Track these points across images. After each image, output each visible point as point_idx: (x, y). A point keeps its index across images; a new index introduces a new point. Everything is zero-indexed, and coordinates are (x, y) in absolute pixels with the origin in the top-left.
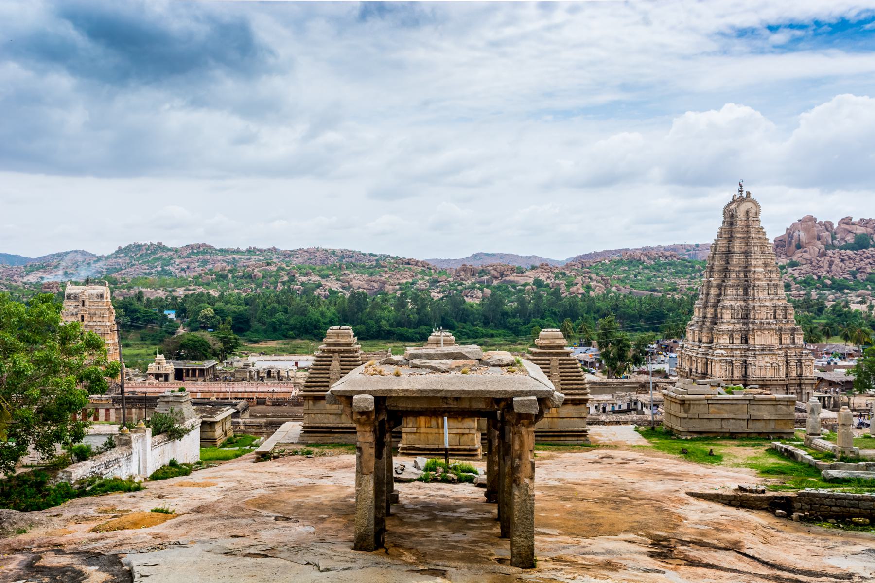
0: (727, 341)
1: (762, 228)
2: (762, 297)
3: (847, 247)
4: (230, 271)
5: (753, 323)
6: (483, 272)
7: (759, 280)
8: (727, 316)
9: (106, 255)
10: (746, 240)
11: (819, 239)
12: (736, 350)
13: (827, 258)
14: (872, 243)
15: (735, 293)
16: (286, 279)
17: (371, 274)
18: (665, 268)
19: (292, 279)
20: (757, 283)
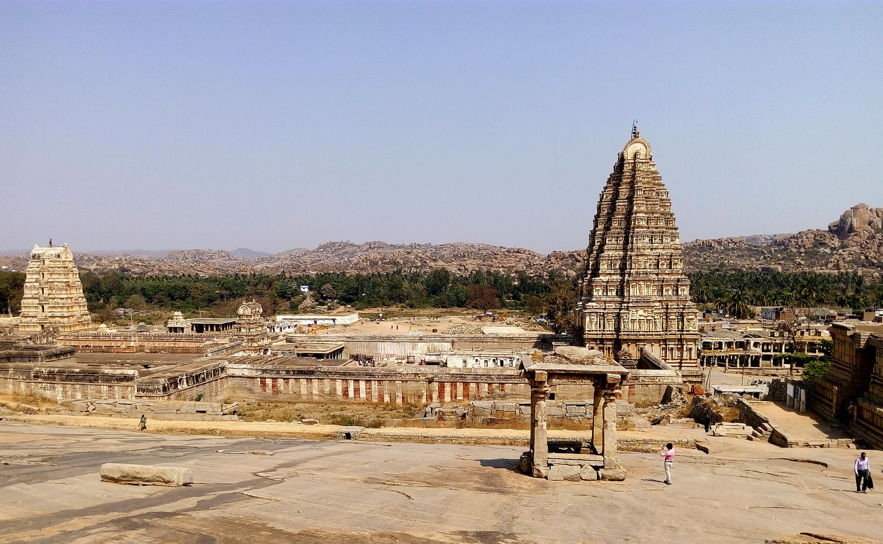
0: (600, 293)
2: (640, 245)
4: (380, 259)
6: (571, 256)
8: (603, 267)
9: (311, 250)
15: (614, 242)
16: (419, 264)
19: (424, 263)
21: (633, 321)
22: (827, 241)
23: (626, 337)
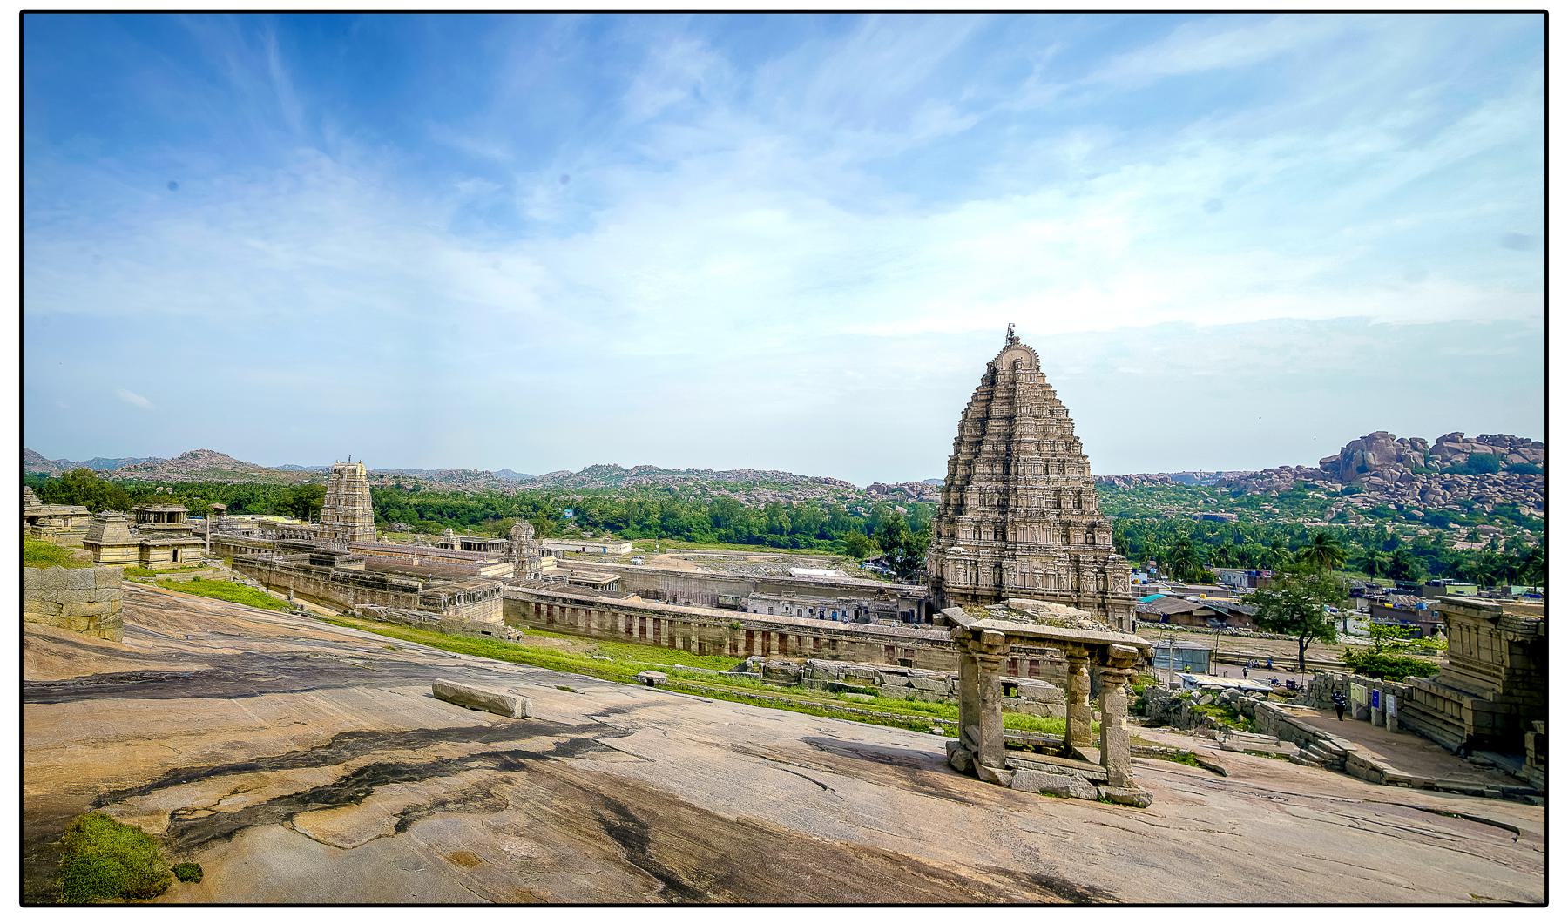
0: (970, 536)
2: (1029, 476)
5: (1014, 512)
8: (972, 500)
15: (988, 470)
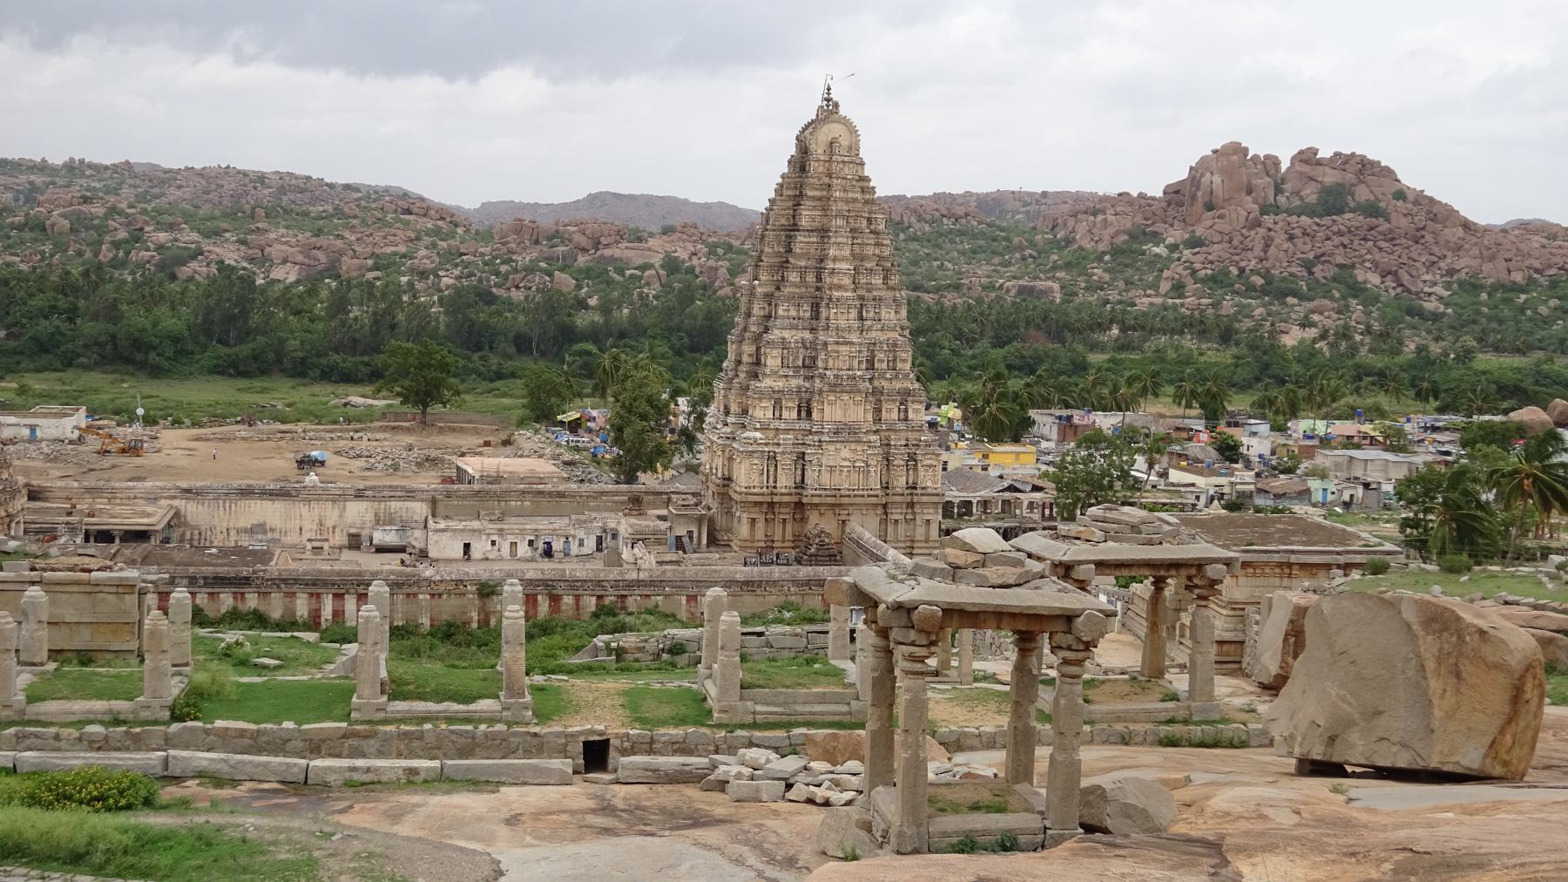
1: (867, 179)
2: (843, 323)
3: (1309, 211)
5: (822, 377)
7: (840, 287)
8: (772, 360)
10: (824, 203)
11: (1249, 192)
12: (787, 431)
13: (1262, 231)
14: (1352, 204)
16: (122, 234)
17: (318, 233)
18: (952, 242)
19: (137, 237)
20: (836, 294)
21: (832, 469)
22: (1159, 227)
23: (816, 500)
